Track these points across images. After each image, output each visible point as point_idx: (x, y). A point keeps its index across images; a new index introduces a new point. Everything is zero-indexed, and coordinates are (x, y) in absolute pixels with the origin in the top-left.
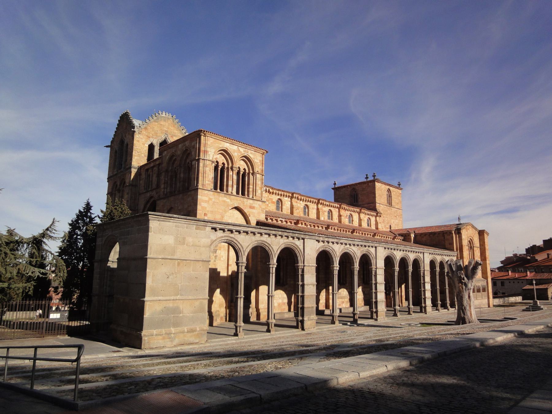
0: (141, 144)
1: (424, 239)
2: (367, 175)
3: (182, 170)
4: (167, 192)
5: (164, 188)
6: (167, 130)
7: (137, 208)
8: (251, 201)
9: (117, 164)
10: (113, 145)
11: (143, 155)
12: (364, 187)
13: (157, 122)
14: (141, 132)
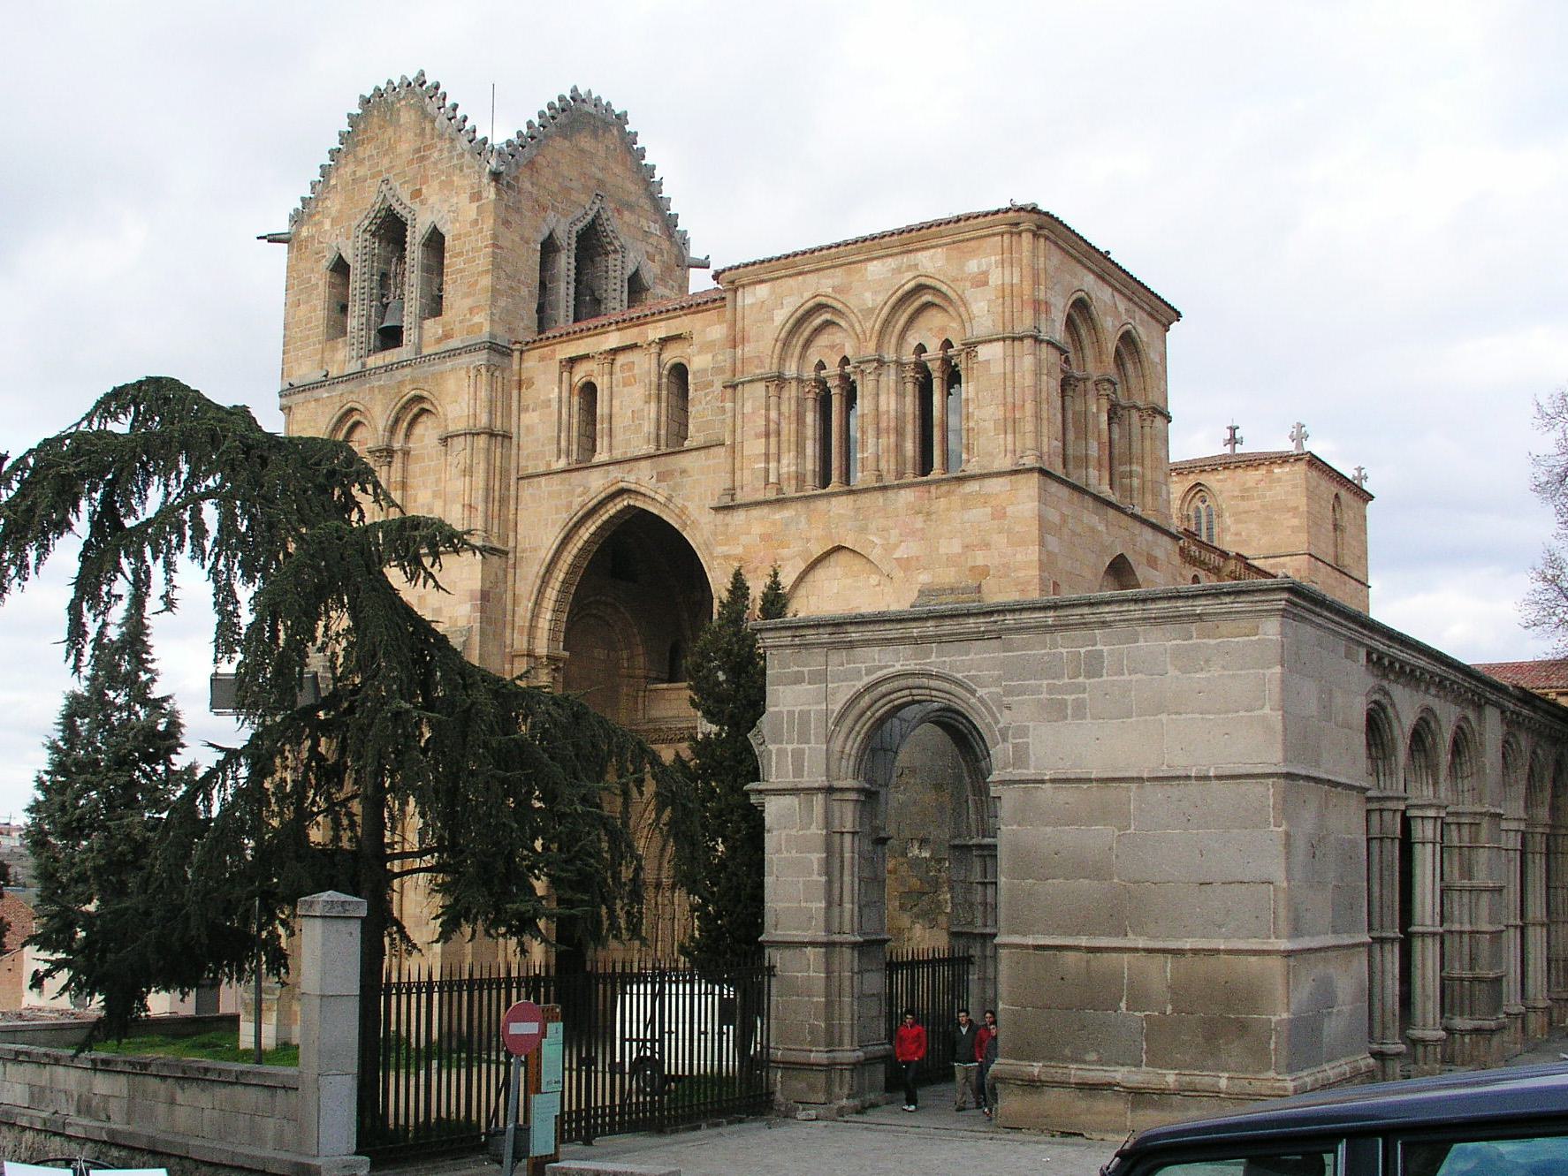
2: (1233, 429)
6: (600, 175)
7: (511, 544)
9: (353, 323)
10: (304, 232)
11: (524, 292)
12: (1251, 484)
14: (516, 178)
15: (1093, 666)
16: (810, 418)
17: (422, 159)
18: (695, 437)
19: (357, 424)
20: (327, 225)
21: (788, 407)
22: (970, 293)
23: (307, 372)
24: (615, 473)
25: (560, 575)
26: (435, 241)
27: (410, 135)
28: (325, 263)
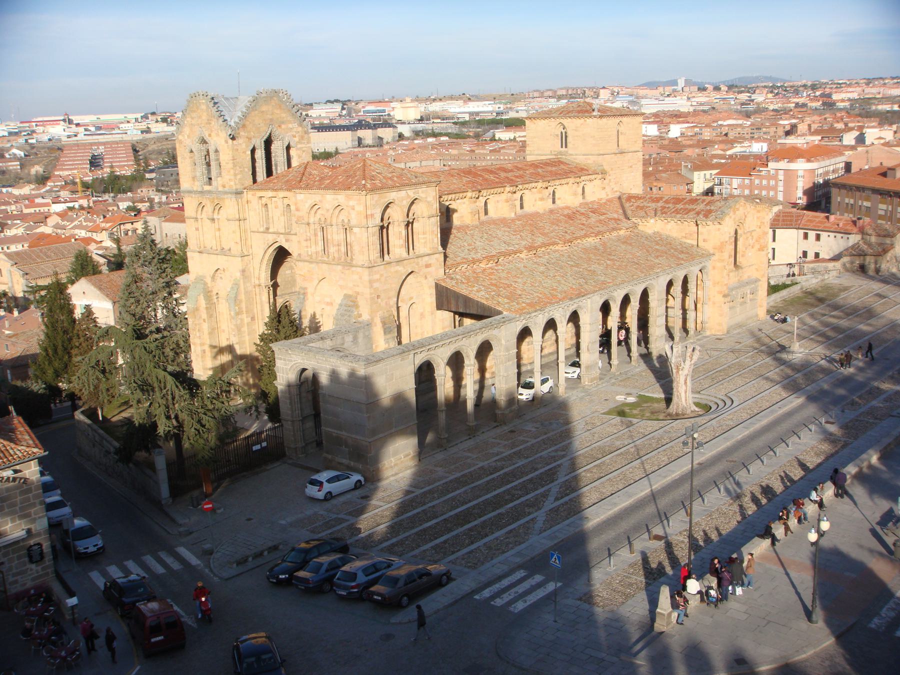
6: (271, 117)
7: (251, 252)
8: (426, 258)
11: (246, 170)
17: (210, 123)
21: (312, 232)
27: (205, 114)
28: (187, 150)
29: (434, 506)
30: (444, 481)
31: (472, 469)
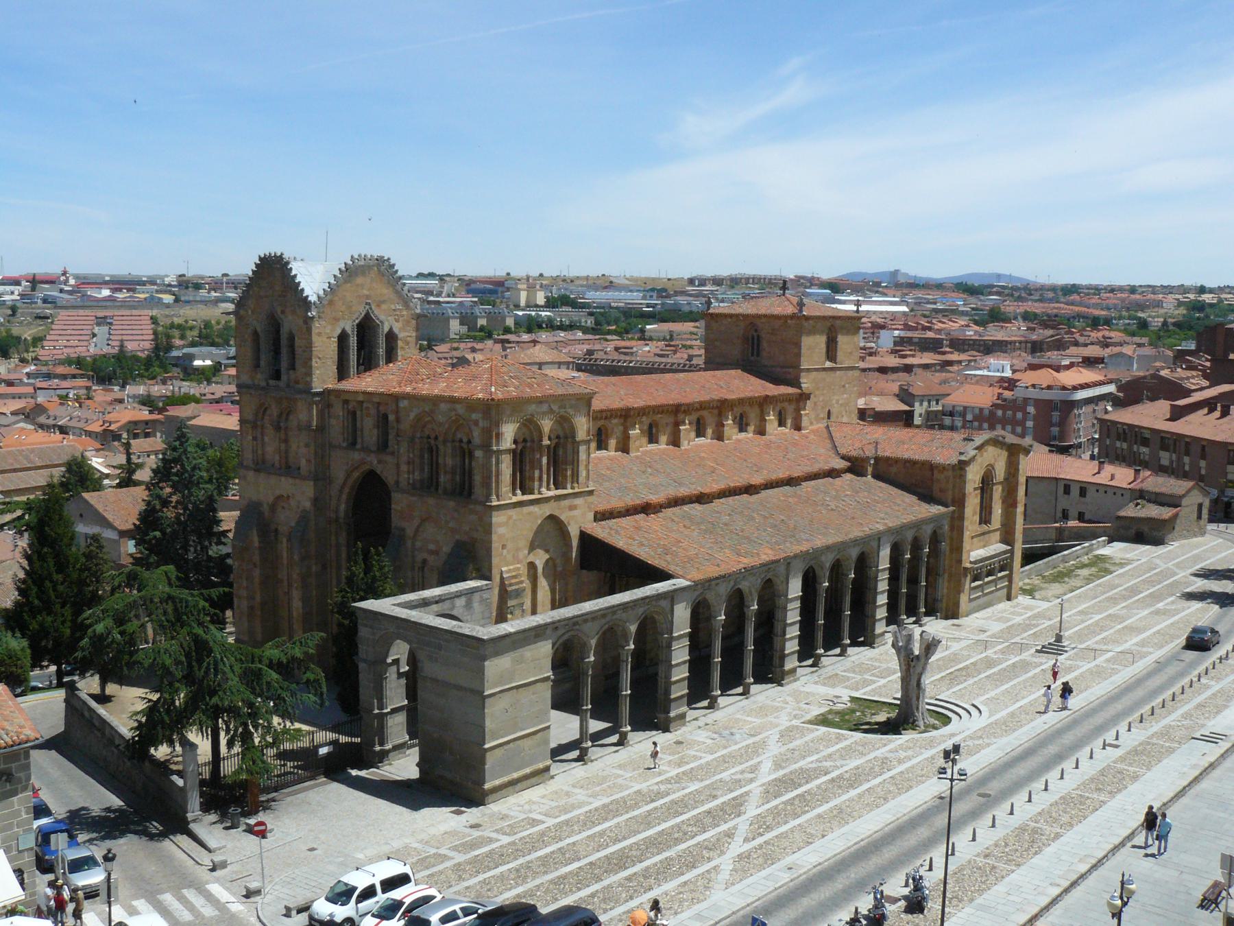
0: (325, 339)
1: (894, 469)
3: (449, 451)
4: (414, 480)
5: (409, 472)
9: (262, 363)
10: (242, 312)
11: (329, 362)
13: (349, 282)
15: (440, 648)
16: (426, 456)
17: (285, 296)
18: (390, 449)
19: (266, 409)
20: (250, 312)
22: (473, 428)
23: (245, 379)
24: (363, 455)
25: (347, 490)
26: (291, 338)
28: (249, 331)
29: (574, 843)
30: (587, 808)
31: (627, 792)
